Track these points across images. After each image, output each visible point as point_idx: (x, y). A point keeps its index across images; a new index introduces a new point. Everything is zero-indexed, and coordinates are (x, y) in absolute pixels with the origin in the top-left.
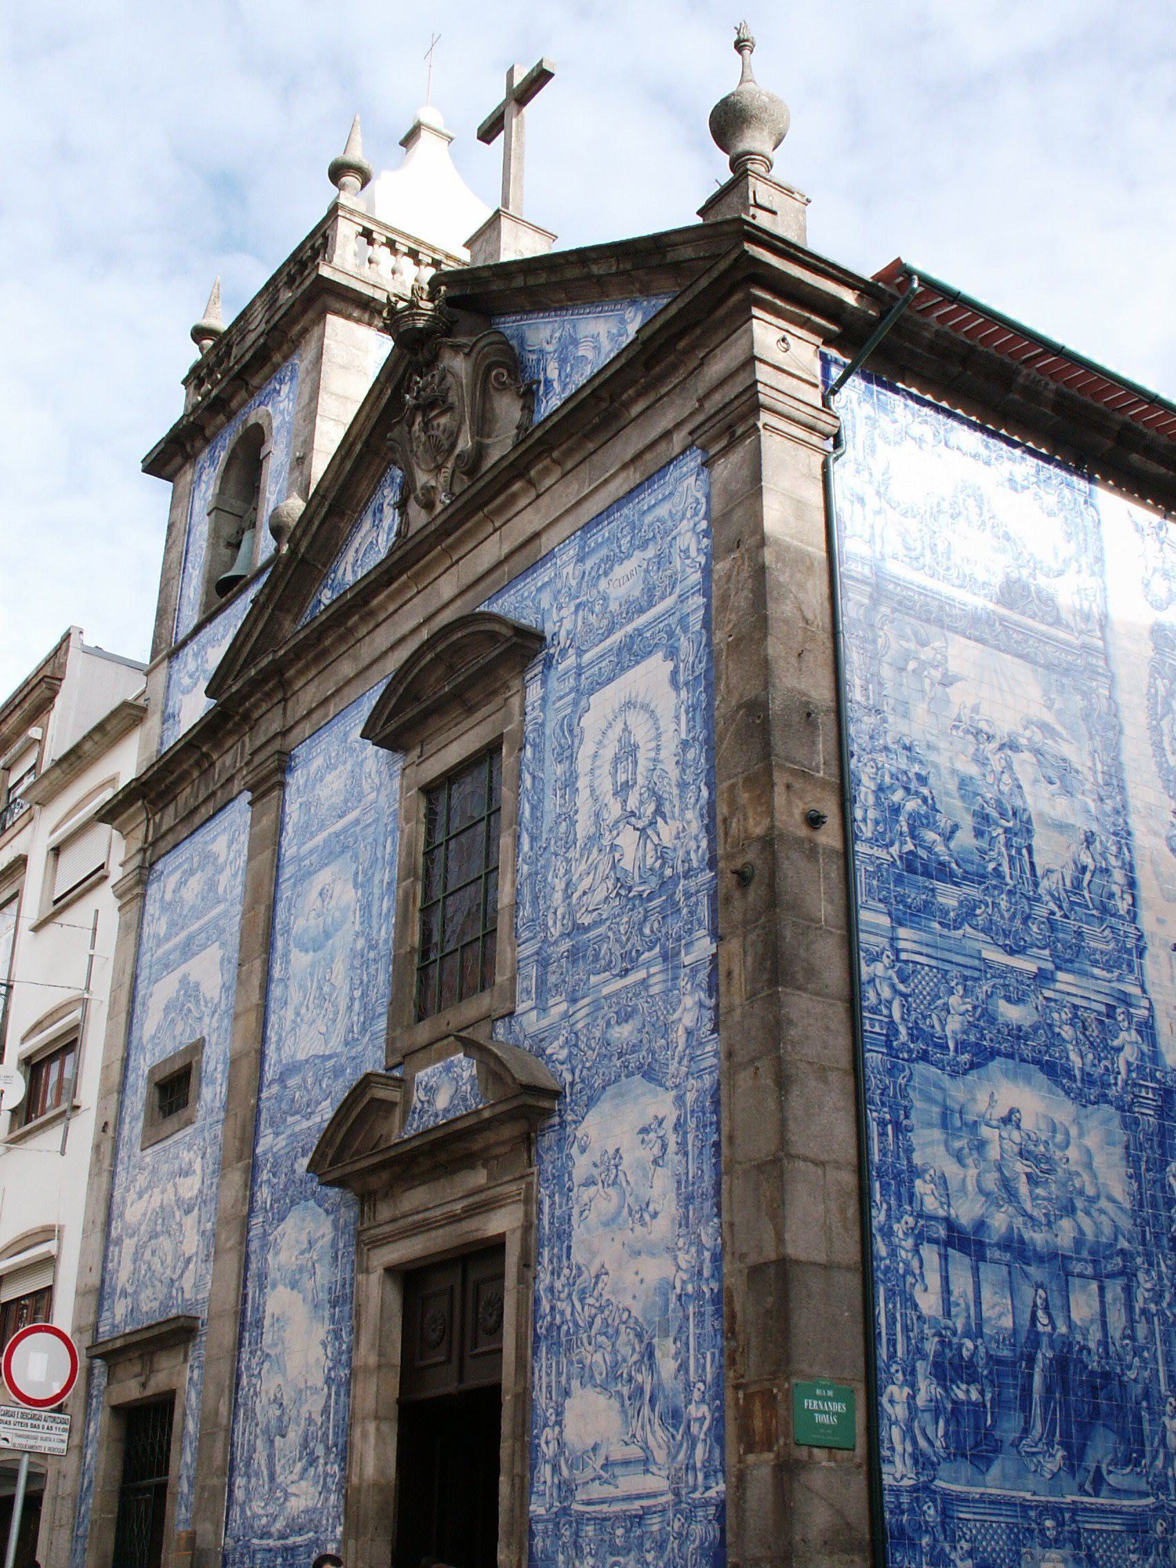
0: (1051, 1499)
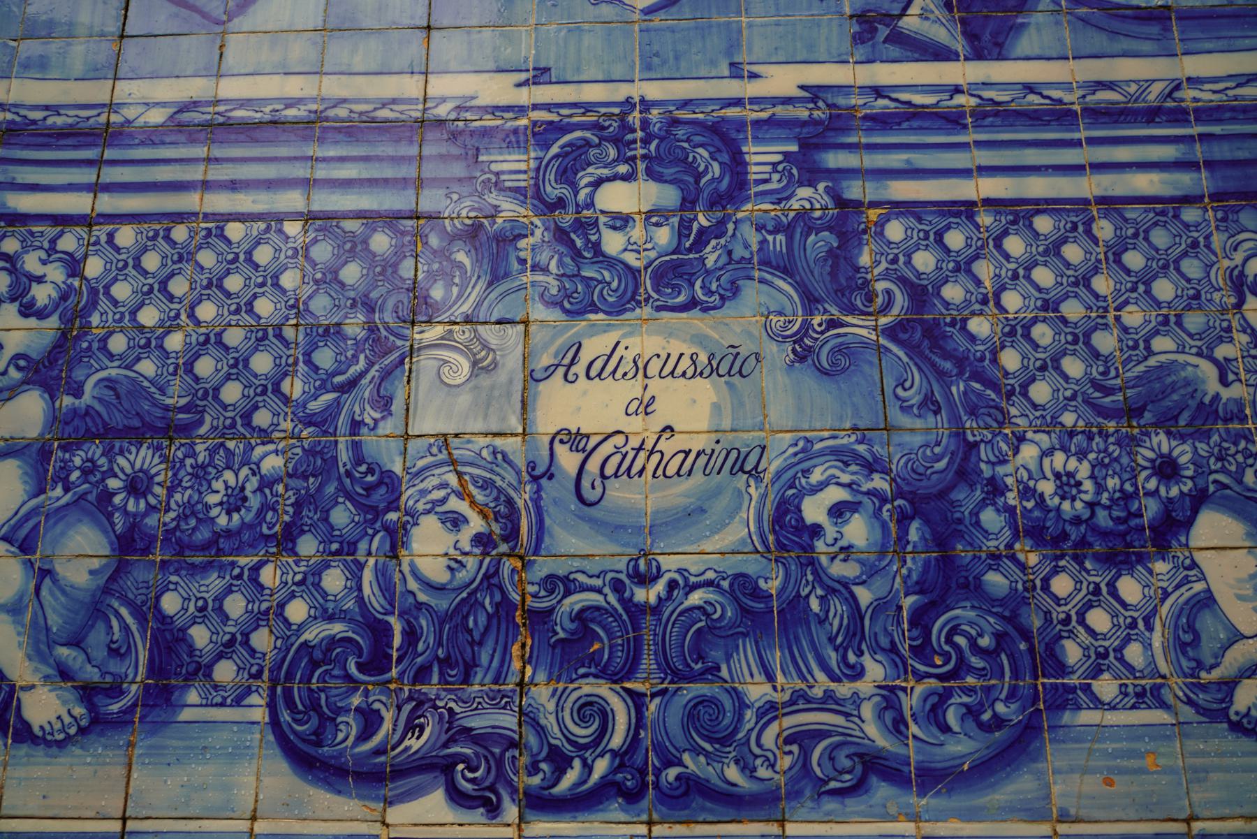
0: (654, 91)
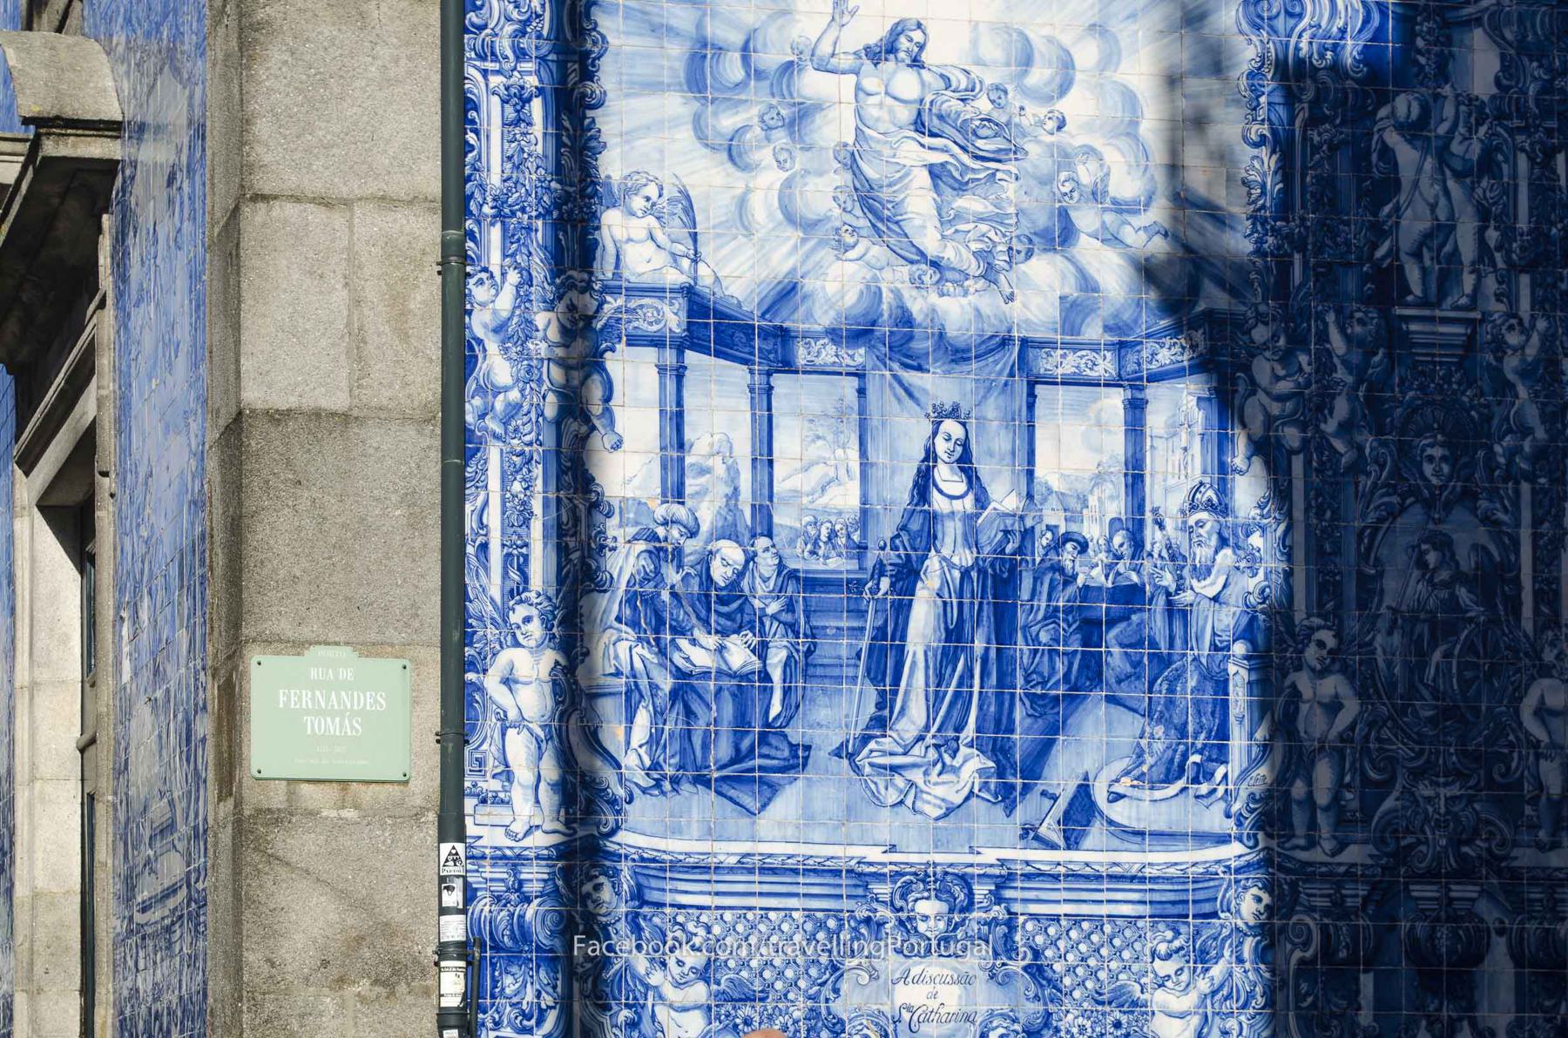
0: (939, 858)
